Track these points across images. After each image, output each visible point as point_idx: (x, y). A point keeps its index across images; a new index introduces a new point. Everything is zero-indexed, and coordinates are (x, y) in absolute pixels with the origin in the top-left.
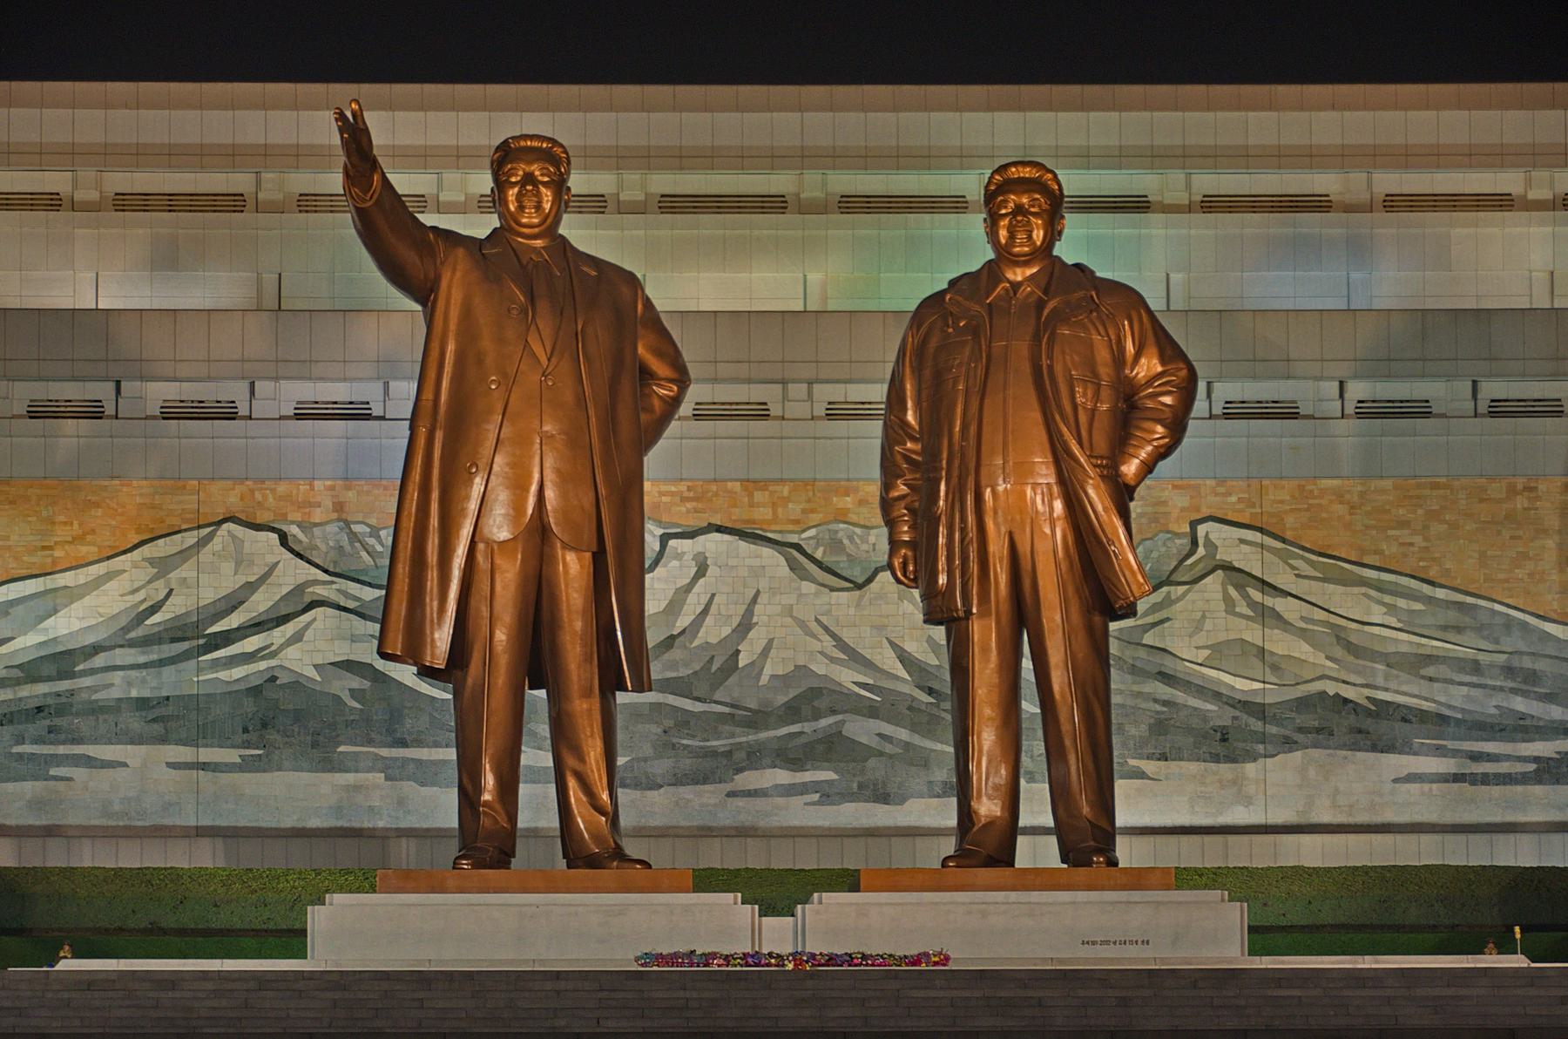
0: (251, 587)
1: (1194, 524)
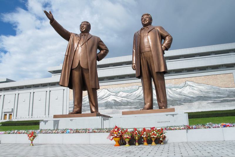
0: (105, 94)
1: (185, 82)
